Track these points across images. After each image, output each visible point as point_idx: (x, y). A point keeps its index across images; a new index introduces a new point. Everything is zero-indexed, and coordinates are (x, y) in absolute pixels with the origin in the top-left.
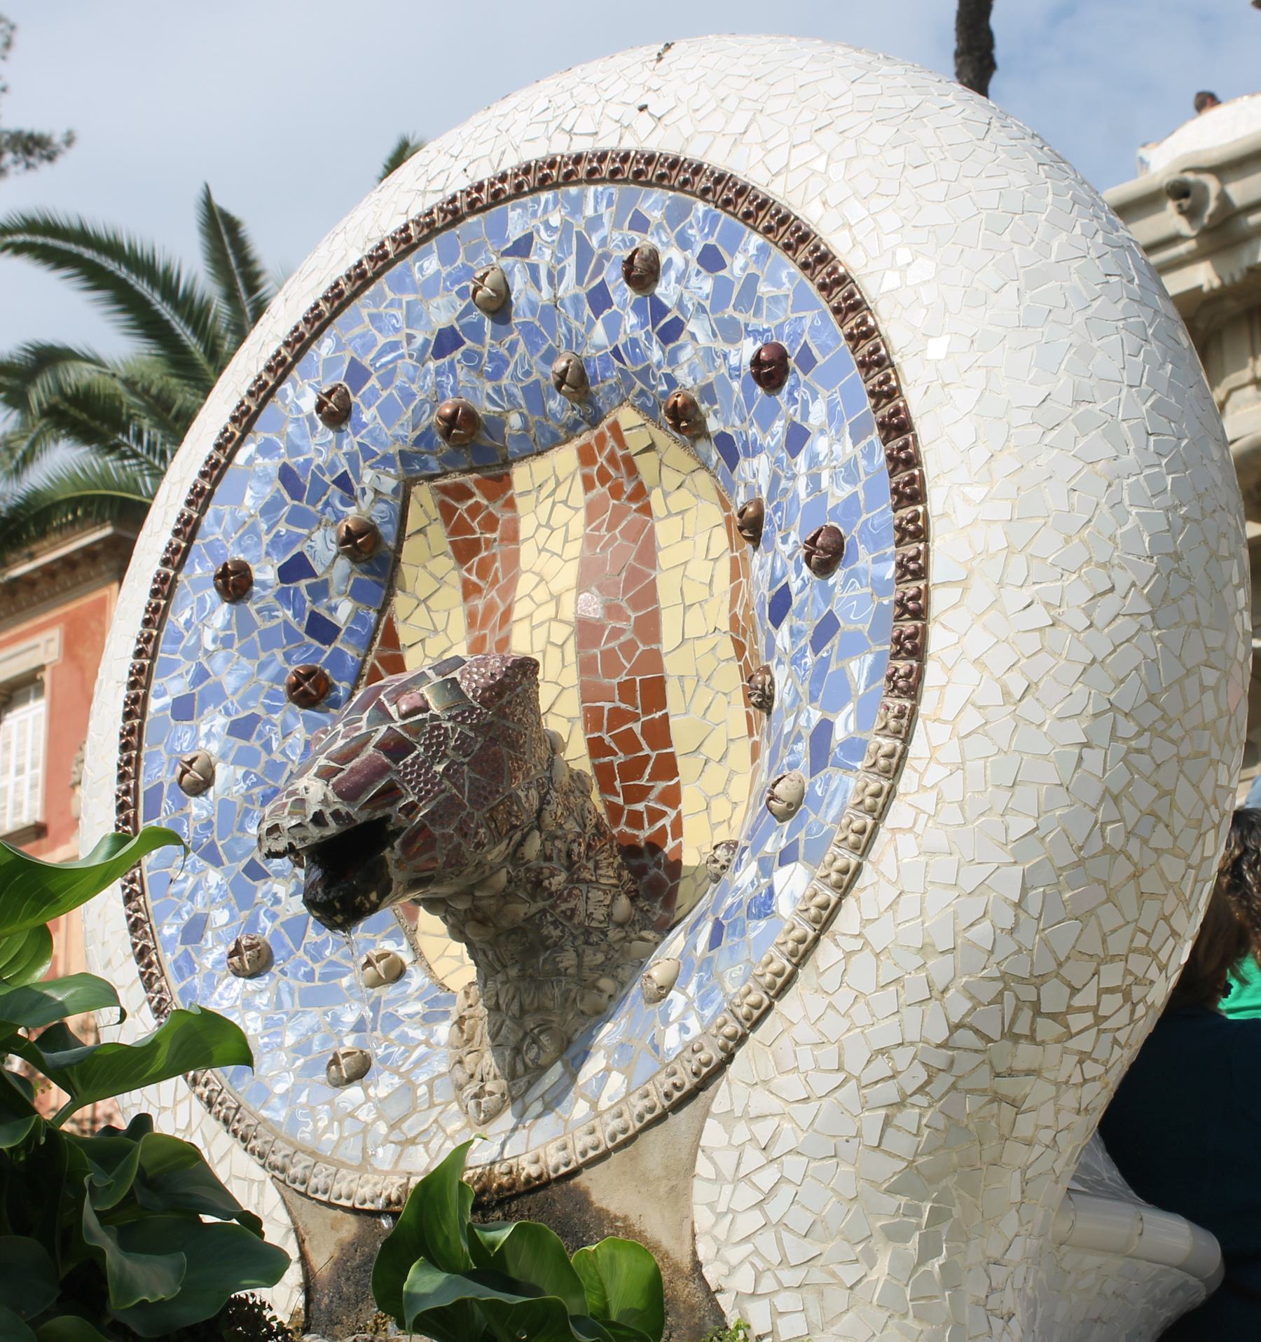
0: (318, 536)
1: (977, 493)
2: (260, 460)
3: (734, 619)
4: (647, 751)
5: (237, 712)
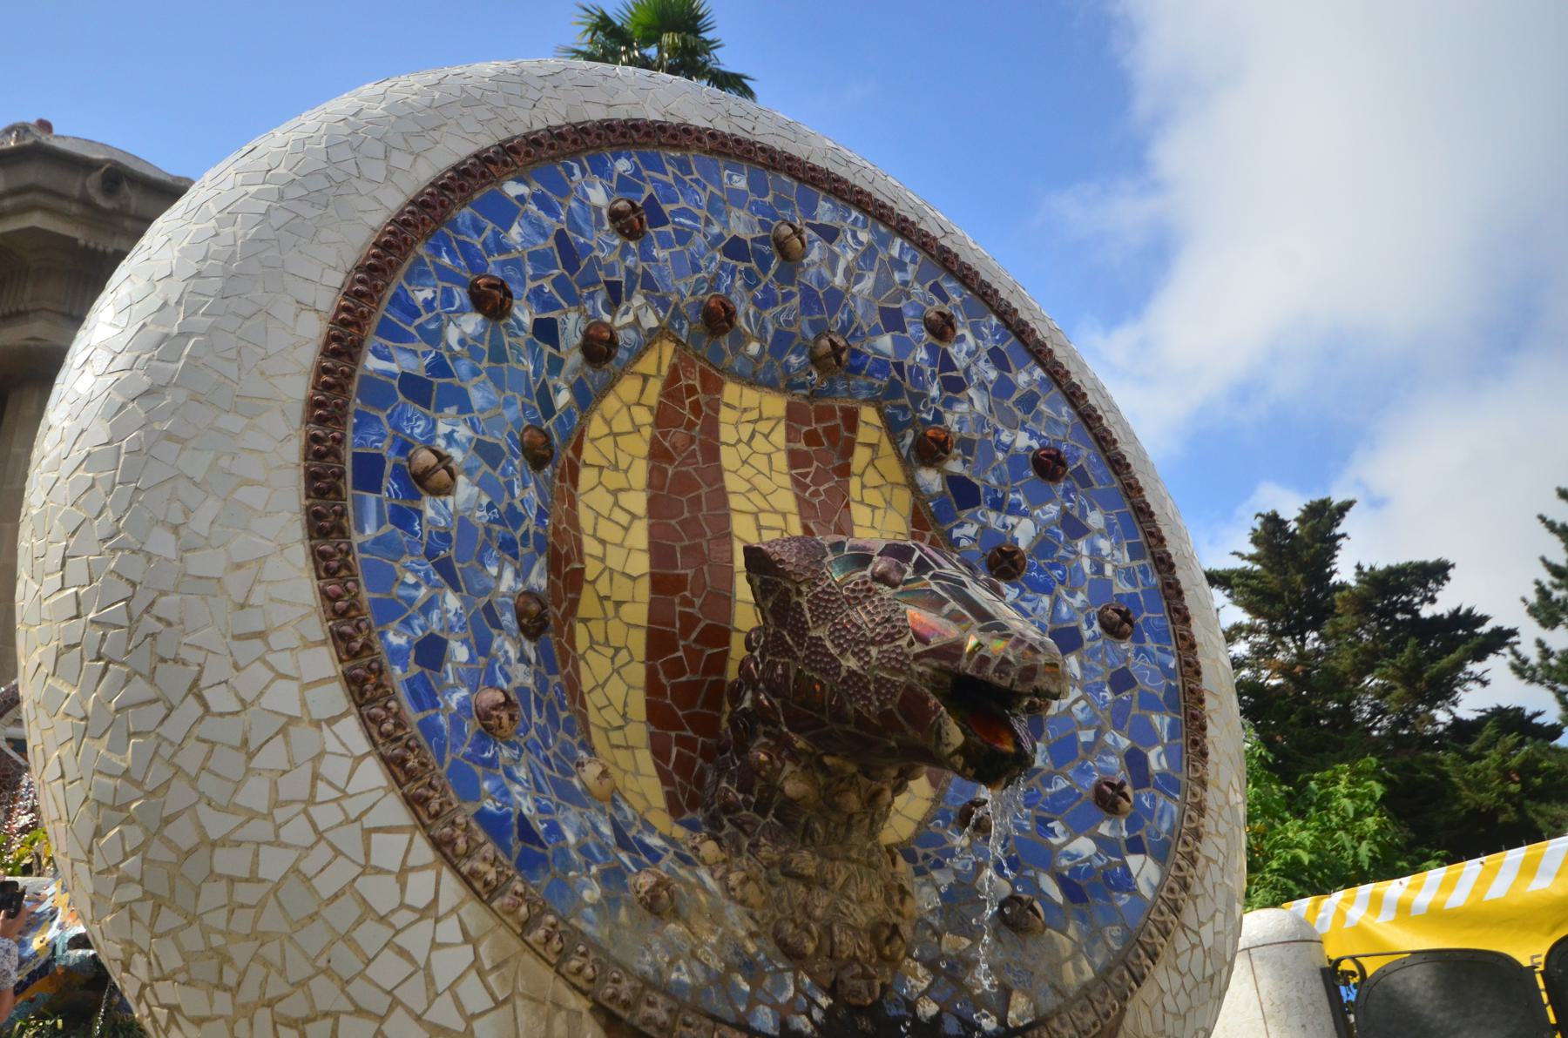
2: (533, 207)
5: (484, 433)
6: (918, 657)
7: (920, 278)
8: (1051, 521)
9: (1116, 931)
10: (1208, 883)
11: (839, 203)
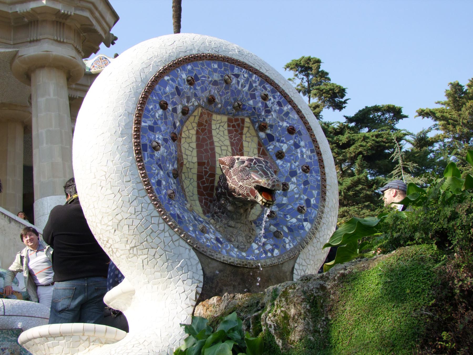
2: (171, 82)
6: (253, 182)
7: (260, 85)
8: (291, 145)
9: (299, 238)
10: (323, 228)
11: (240, 67)
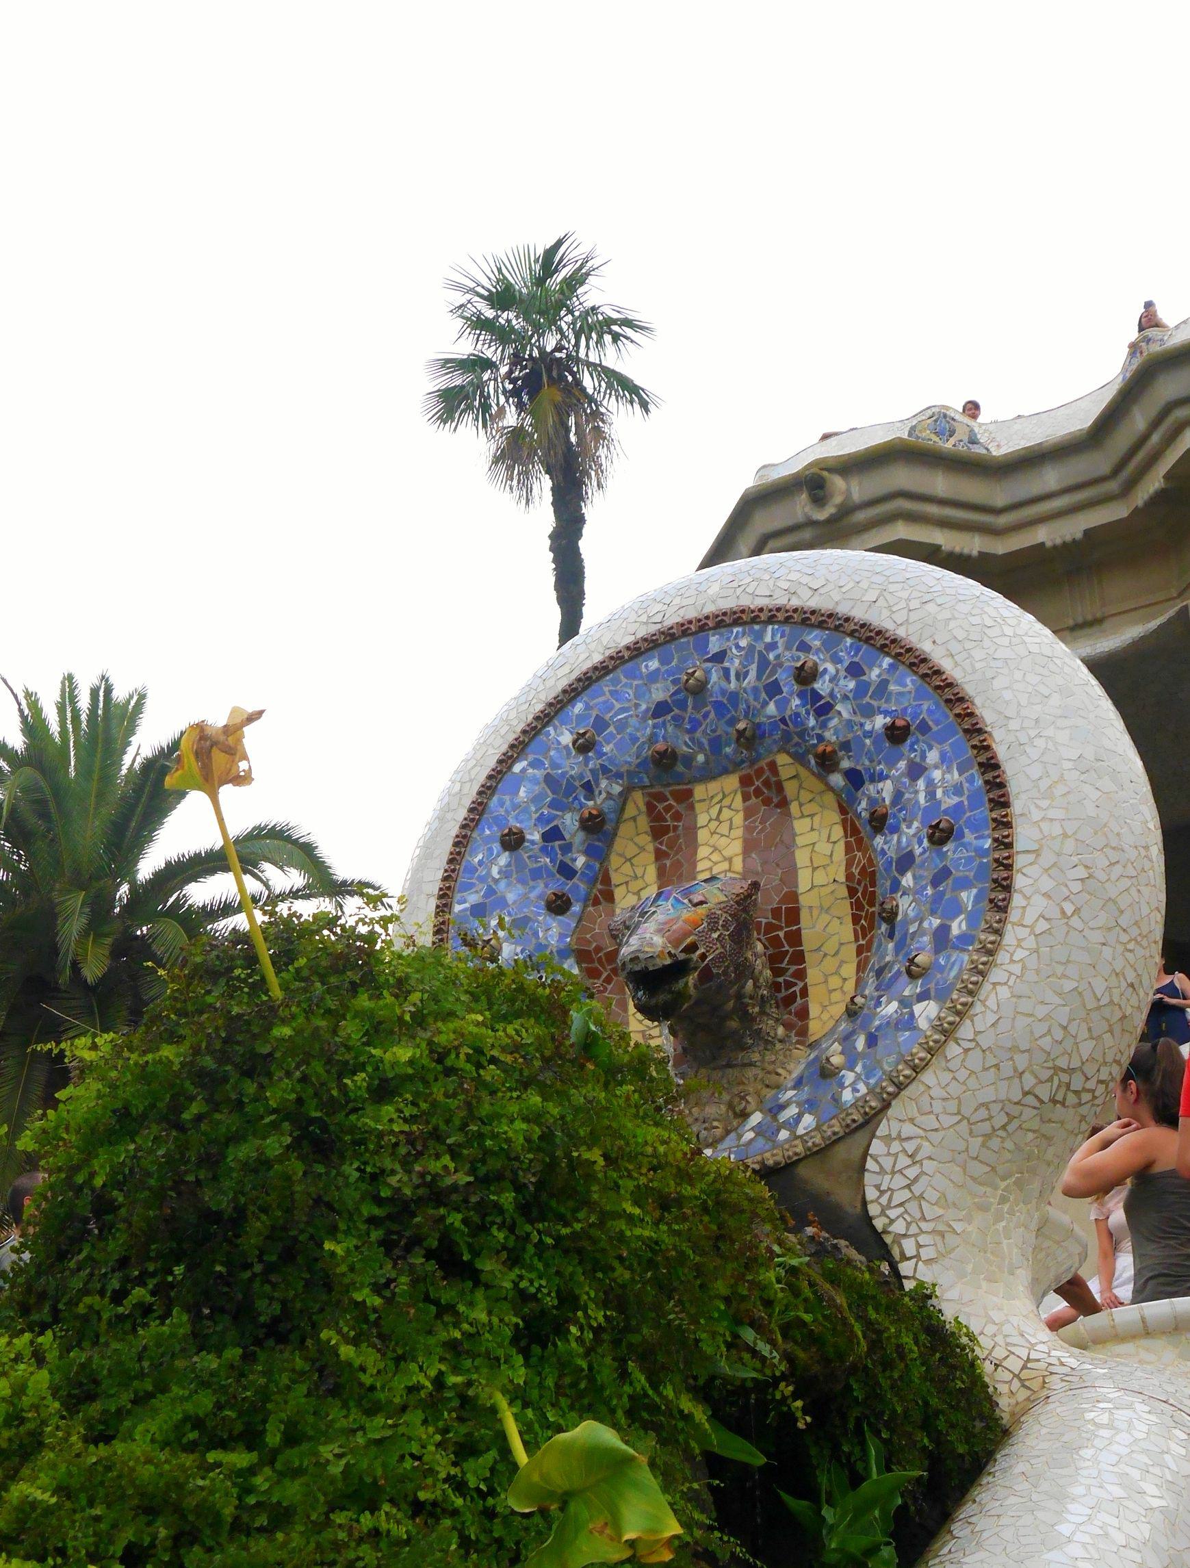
0: (568, 816)
1: (1044, 803)
2: (531, 771)
3: (849, 877)
4: (787, 948)
8: (902, 775)
11: (723, 630)
